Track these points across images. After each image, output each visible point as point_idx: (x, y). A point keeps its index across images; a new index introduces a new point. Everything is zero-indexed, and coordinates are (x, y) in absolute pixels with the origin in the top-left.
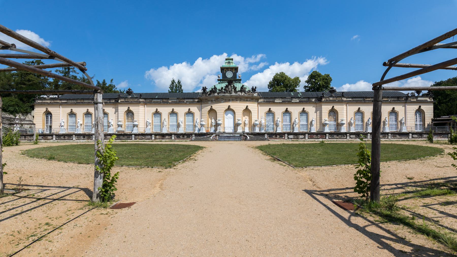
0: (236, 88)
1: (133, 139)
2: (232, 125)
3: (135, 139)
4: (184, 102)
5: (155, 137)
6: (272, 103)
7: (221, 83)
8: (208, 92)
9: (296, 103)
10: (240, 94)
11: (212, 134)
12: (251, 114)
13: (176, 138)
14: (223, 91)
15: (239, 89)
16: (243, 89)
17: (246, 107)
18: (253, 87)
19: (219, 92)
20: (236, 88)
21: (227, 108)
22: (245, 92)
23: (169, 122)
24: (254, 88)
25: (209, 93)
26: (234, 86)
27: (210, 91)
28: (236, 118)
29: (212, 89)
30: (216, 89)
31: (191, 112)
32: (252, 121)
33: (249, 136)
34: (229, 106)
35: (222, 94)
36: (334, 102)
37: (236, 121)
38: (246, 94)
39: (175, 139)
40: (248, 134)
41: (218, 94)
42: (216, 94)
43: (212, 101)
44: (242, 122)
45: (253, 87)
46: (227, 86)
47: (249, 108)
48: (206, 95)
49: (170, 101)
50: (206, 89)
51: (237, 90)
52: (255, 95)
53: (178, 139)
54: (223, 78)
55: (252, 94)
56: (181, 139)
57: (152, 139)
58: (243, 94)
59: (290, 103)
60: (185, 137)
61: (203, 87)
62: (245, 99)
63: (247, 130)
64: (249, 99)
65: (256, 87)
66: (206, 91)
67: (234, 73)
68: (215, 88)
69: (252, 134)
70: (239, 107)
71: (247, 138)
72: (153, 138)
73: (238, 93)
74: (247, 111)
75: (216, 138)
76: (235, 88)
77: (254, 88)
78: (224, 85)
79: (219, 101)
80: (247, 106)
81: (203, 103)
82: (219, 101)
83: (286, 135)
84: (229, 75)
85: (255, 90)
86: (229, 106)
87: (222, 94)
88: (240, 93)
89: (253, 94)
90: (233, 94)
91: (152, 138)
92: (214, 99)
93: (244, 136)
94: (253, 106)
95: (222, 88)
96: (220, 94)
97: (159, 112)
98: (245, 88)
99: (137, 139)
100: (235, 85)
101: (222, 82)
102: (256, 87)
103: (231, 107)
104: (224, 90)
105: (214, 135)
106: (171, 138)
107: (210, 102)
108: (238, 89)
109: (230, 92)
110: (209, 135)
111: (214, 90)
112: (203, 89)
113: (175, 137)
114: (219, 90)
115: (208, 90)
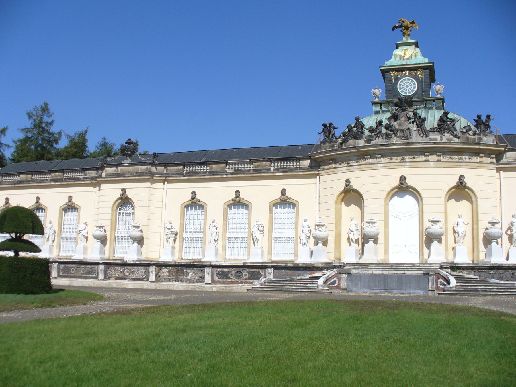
1: (101, 276)
3: (105, 278)
4: (269, 170)
5: (156, 275)
7: (383, 111)
10: (436, 139)
12: (477, 201)
13: (216, 279)
14: (384, 131)
15: (436, 125)
17: (457, 180)
18: (479, 117)
19: (372, 136)
20: (424, 120)
21: (396, 183)
22: (452, 130)
23: (225, 230)
24: (484, 118)
25: (340, 141)
26: (415, 114)
27: (344, 134)
28: (426, 217)
29: (350, 128)
30: (363, 126)
31: (290, 198)
32: (480, 226)
33: (456, 277)
34: (403, 178)
35: (380, 140)
37: (427, 224)
38: (458, 138)
39: (213, 281)
40: (454, 267)
41: (368, 141)
42: (361, 142)
44: (446, 229)
45: (479, 117)
47: (469, 182)
48: (333, 146)
49: (230, 169)
50: (334, 128)
52: (489, 140)
53: (224, 283)
54: (387, 97)
55: (477, 137)
56: (232, 282)
57: (148, 280)
58: (448, 139)
61: (325, 125)
65: (488, 117)
66: (333, 135)
67: (422, 82)
71: (449, 282)
72: (152, 277)
73: (432, 136)
75: (339, 281)
76: (420, 122)
77: (484, 118)
79: (370, 164)
80: (461, 177)
81: (323, 172)
82: (370, 164)
85: (488, 127)
86: (403, 178)
88: (437, 136)
89: (480, 139)
90: (416, 138)
91: (149, 275)
93: (439, 275)
95: (380, 123)
96: (373, 143)
97: (199, 200)
98: (453, 120)
99: (109, 279)
101: (384, 109)
102: (488, 117)
103: (410, 182)
104: (387, 127)
106: (202, 278)
107: (343, 168)
109: (406, 134)
112: (323, 131)
113: (213, 276)
114: (371, 130)
115: (338, 133)
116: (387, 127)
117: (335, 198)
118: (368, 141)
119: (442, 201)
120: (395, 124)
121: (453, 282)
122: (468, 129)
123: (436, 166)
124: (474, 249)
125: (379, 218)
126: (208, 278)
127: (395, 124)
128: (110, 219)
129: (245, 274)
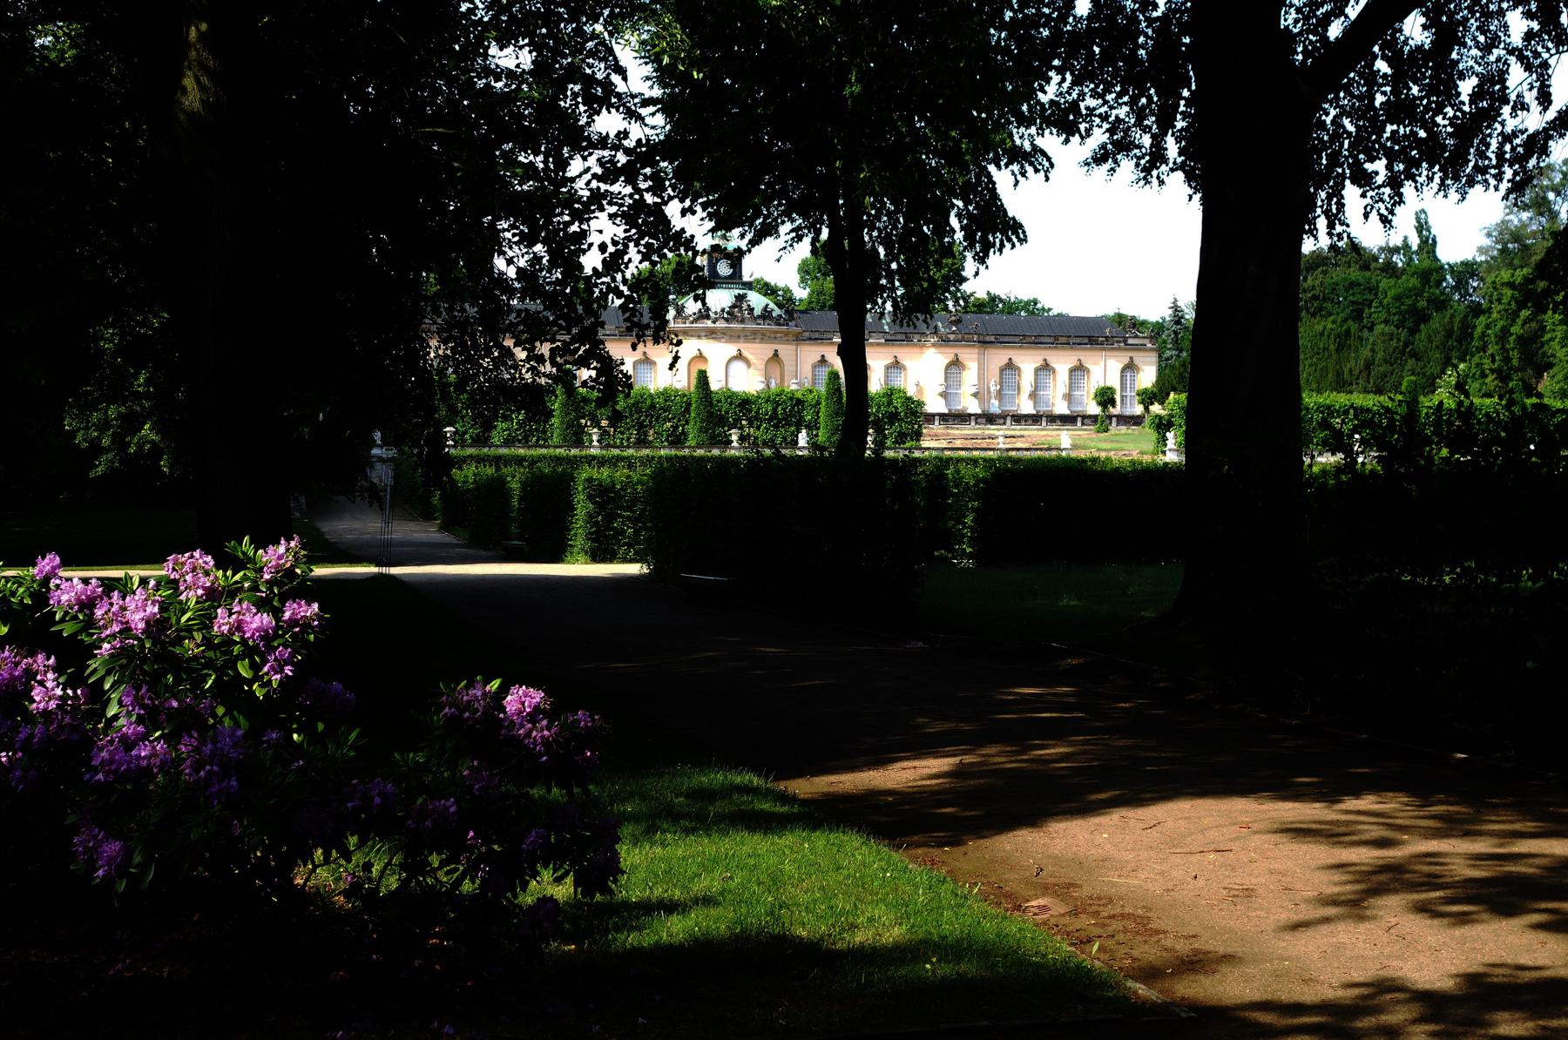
0: (752, 310)
8: (687, 318)
9: (878, 344)
14: (726, 316)
21: (735, 353)
25: (691, 319)
26: (749, 306)
27: (695, 314)
41: (714, 322)
42: (709, 323)
62: (772, 335)
64: (779, 335)
76: (751, 310)
92: (704, 334)
95: (723, 310)
96: (718, 324)
100: (750, 303)
104: (728, 313)
114: (716, 313)
116: (728, 313)
118: (714, 322)
122: (780, 316)
123: (760, 343)
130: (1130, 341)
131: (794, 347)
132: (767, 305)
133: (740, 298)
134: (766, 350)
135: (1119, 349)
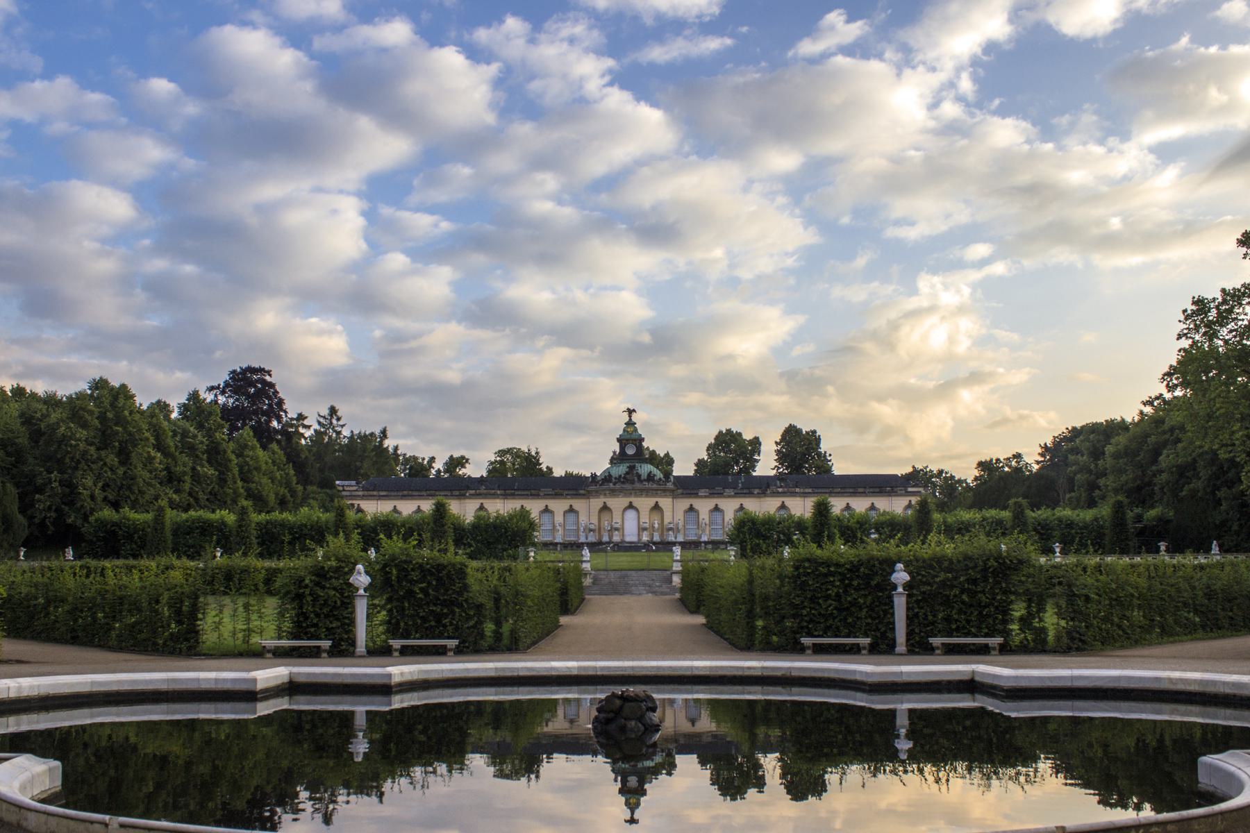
2: (635, 530)
6: (694, 497)
8: (598, 482)
9: (729, 497)
11: (609, 543)
15: (646, 478)
16: (650, 477)
21: (627, 504)
29: (605, 477)
34: (631, 503)
36: (784, 494)
40: (654, 543)
41: (614, 484)
42: (611, 484)
43: (605, 494)
46: (627, 473)
47: (661, 505)
51: (642, 478)
52: (670, 485)
59: (720, 495)
60: (574, 547)
63: (657, 538)
68: (610, 476)
69: (659, 543)
70: (645, 503)
74: (656, 507)
76: (639, 476)
78: (622, 469)
83: (703, 544)
84: (631, 451)
86: (631, 503)
87: (618, 486)
94: (665, 503)
95: (620, 476)
98: (654, 475)
100: (639, 471)
103: (634, 504)
105: (611, 545)
107: (602, 496)
108: (644, 476)
110: (604, 544)
111: (607, 478)
114: (616, 478)
116: (624, 478)
117: (597, 511)
118: (614, 484)
119: (648, 513)
120: (628, 476)
121: (654, 548)
122: (660, 479)
124: (662, 535)
125: (619, 521)
126: (559, 549)
127: (628, 476)
128: (375, 502)
129: (574, 547)
130: (910, 489)
131: (670, 500)
132: (651, 472)
133: (632, 468)
134: (650, 502)
135: (901, 495)
